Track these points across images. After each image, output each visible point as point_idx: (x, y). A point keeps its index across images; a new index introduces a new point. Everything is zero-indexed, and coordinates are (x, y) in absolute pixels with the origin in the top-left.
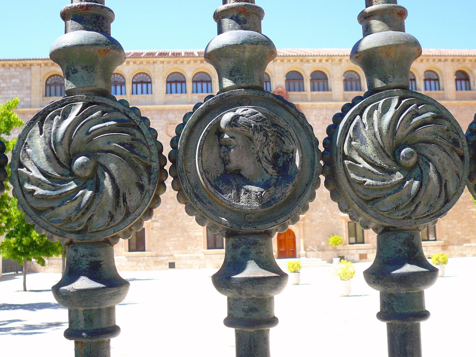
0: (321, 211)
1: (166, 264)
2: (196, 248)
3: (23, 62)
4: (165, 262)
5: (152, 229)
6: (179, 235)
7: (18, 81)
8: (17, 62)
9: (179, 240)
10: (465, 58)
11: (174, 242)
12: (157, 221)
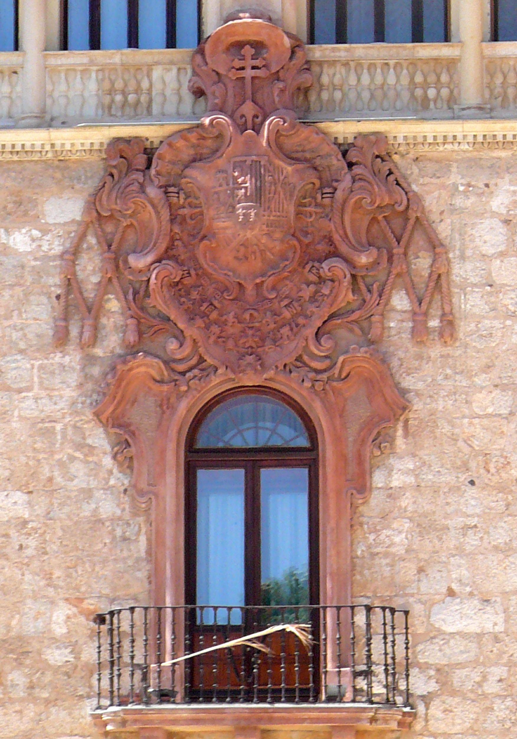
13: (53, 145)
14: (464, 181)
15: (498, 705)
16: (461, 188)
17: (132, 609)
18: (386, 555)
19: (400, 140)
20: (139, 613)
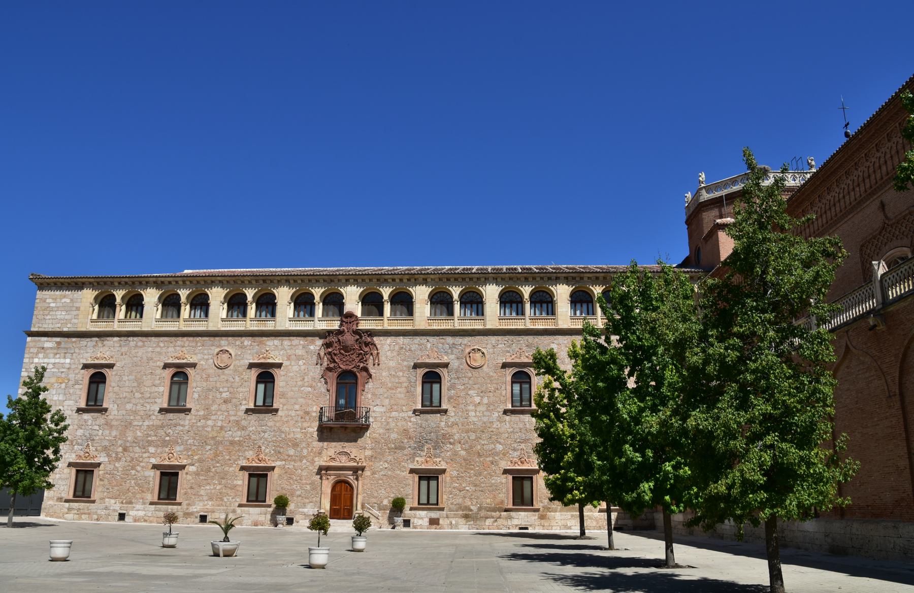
0: (386, 461)
1: (196, 517)
2: (234, 500)
3: (75, 280)
4: (196, 515)
5: (187, 474)
6: (216, 482)
7: (68, 301)
8: (69, 281)
9: (215, 489)
10: (582, 275)
11: (209, 491)
12: (193, 465)
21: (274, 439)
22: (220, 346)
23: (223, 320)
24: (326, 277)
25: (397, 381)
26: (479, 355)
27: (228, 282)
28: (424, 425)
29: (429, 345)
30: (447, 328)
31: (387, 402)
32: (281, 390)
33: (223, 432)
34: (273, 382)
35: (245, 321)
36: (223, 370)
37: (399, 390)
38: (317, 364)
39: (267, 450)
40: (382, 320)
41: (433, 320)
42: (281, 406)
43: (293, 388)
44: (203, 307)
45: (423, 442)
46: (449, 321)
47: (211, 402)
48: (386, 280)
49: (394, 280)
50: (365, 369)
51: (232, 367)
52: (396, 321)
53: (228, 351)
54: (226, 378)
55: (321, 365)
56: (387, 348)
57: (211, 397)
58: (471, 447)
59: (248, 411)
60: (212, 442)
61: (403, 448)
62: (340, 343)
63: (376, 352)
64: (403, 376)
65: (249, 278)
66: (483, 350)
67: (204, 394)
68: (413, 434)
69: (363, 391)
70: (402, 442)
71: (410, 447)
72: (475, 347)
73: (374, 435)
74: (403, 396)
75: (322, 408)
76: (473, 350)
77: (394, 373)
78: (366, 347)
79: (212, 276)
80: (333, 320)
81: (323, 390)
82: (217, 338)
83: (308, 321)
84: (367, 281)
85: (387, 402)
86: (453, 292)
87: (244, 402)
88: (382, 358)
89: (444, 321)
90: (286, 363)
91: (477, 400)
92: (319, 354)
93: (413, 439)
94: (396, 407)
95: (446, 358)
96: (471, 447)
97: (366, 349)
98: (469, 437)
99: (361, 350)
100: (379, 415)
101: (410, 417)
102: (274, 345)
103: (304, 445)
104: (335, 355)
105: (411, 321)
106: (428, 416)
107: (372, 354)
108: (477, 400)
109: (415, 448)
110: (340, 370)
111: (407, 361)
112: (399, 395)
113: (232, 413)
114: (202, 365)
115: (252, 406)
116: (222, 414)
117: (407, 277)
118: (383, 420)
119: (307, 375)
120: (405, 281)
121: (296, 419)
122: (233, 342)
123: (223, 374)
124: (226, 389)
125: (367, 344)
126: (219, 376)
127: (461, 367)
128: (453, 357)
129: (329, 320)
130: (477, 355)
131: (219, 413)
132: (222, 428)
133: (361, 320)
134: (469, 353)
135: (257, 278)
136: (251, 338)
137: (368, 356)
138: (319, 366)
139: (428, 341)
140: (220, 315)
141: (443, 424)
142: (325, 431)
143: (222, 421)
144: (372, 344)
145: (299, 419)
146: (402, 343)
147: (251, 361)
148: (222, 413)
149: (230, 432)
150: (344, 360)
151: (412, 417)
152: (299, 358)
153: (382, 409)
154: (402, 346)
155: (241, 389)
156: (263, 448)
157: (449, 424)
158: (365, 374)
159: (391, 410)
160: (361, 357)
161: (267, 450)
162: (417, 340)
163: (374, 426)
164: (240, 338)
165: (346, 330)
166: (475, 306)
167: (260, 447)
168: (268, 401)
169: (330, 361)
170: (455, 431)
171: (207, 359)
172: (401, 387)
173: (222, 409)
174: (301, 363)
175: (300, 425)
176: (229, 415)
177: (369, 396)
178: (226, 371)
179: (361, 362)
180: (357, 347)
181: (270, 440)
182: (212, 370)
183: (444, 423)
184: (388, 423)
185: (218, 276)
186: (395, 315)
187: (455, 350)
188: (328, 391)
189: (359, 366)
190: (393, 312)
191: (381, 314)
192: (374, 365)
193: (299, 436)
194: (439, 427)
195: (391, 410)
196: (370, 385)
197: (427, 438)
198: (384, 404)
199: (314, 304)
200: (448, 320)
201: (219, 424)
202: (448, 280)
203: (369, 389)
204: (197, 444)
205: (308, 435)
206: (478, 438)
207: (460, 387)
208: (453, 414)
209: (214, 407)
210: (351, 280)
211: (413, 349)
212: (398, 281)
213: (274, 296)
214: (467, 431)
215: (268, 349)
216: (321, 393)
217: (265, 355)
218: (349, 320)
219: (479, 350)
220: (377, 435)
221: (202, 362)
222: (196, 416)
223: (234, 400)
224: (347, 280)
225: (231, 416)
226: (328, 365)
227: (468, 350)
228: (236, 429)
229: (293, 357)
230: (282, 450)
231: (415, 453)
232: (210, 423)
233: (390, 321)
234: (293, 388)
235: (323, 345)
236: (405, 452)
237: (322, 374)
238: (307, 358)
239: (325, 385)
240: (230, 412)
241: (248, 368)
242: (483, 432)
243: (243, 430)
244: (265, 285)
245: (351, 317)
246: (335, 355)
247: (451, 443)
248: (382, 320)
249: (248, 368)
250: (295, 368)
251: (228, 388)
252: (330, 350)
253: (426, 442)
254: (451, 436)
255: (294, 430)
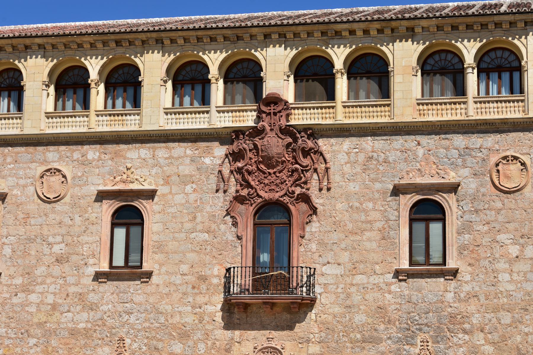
13: (216, 133)
14: (335, 142)
15: (341, 295)
16: (334, 144)
17: (238, 267)
18: (310, 251)
19: (316, 130)
20: (240, 269)
21: (147, 324)
22: (45, 162)
23: (49, 116)
24: (228, 32)
25: (363, 218)
26: (515, 167)
27: (54, 46)
28: (414, 299)
29: (420, 152)
30: (454, 118)
31: (345, 257)
32: (155, 238)
33: (57, 314)
34: (142, 224)
35: (87, 116)
36: (53, 205)
37: (368, 234)
38: (217, 191)
39: (135, 345)
40: (333, 107)
41: (427, 104)
42: (157, 266)
43: (177, 235)
44: (13, 93)
45: (414, 329)
46: (458, 106)
47: (34, 261)
48: (338, 33)
49: (352, 32)
50: (305, 198)
51: (67, 199)
52: (359, 109)
53: (59, 171)
54: (58, 218)
55: (225, 192)
56: (342, 158)
57: (33, 253)
58: (504, 338)
59: (98, 276)
60: (39, 332)
61: (380, 341)
62: (258, 153)
63: (323, 166)
64: (374, 209)
65: (91, 39)
66: (524, 158)
67: (22, 247)
68: (394, 316)
69: (303, 237)
70: (376, 330)
71: (389, 338)
72: (508, 153)
73: (323, 317)
74: (374, 245)
75: (228, 270)
76: (505, 158)
77: (357, 204)
78: (305, 157)
79: (26, 37)
80: (243, 111)
81: (231, 237)
82: (40, 149)
83: (199, 113)
84: (304, 35)
85: (345, 257)
86: (464, 51)
87: (91, 261)
88: (335, 177)
89: (448, 106)
90: (162, 190)
91: (514, 250)
92: (220, 172)
93: (394, 324)
94: (362, 266)
95: (452, 174)
96: (504, 338)
97: (306, 162)
98: (499, 320)
99: (297, 163)
100: (332, 281)
101: (388, 284)
102: (139, 157)
103: (199, 335)
104: (250, 173)
105: (387, 108)
106: (422, 282)
107: (316, 170)
108: (514, 250)
109: (399, 340)
110: (260, 200)
111: (381, 182)
112: (368, 245)
113: (71, 280)
114: (16, 196)
115: (105, 267)
116: (55, 283)
117: (377, 25)
118: (339, 290)
119: (201, 211)
120: (374, 33)
121: (183, 288)
122: (68, 154)
123: (53, 211)
124: (59, 239)
125: (306, 153)
126: (45, 215)
127: (482, 190)
128: (466, 172)
129: (236, 111)
130: (512, 167)
131: (48, 281)
132: (54, 307)
133: (294, 108)
134: (497, 165)
135: (105, 38)
136: (98, 146)
137: (308, 174)
138: (221, 194)
139: (419, 144)
140: (44, 107)
141: (450, 296)
142: (236, 310)
143: (55, 294)
144: (315, 153)
145: (189, 289)
146: (370, 149)
147: (101, 188)
148: (54, 280)
149: (70, 315)
150: (266, 181)
151: (391, 284)
152: (185, 180)
153: (339, 271)
154: (370, 154)
155: (85, 238)
156: (128, 341)
157: (462, 295)
158: (303, 206)
159: (354, 271)
160: (296, 175)
161: (135, 345)
162: (399, 141)
163: (323, 300)
164: (79, 147)
165: (268, 128)
166: (506, 76)
167: (122, 339)
168: (134, 258)
169: (241, 185)
170: (472, 308)
171: (25, 186)
172: (371, 230)
173: (54, 274)
174: (189, 188)
175: (191, 299)
176: (66, 284)
177: (314, 246)
178: (58, 206)
179: (297, 185)
180: (288, 157)
181: (140, 328)
182: (35, 206)
183: (452, 294)
184: (348, 296)
185: (37, 36)
186: (357, 97)
187: (469, 159)
188: (239, 238)
189: (293, 192)
190: (353, 92)
191: (331, 96)
192: (321, 190)
193: (189, 319)
194: (442, 302)
195: (354, 271)
196: (314, 227)
197: (420, 322)
198: (341, 261)
199: (209, 81)
200: (455, 103)
201: (50, 299)
202: (454, 28)
203: (312, 233)
204: (13, 336)
205: (206, 318)
206: (516, 323)
207: (480, 228)
208: (468, 278)
209: (41, 270)
210: (273, 36)
211: (391, 159)
212: (360, 33)
213: (136, 70)
214: (496, 310)
215: (129, 165)
216: (227, 243)
217: (125, 176)
218: (272, 109)
219: (516, 158)
220: (330, 318)
221: (15, 192)
222: (8, 286)
223: (74, 258)
224: (267, 36)
225: (70, 285)
226: (237, 191)
227: (494, 159)
228: (79, 308)
229: (174, 178)
230: (160, 345)
231: (399, 350)
232: (33, 298)
233: (347, 110)
234: (177, 235)
235: (226, 155)
236: (382, 347)
237: (226, 208)
238: (200, 180)
239: (233, 229)
240: (68, 278)
241: (96, 200)
242: (526, 310)
243: (92, 309)
244: (120, 50)
245: (276, 103)
246: (250, 173)
247: (465, 332)
248: (333, 107)
249: (96, 200)
250: (179, 199)
251: (63, 236)
252: (240, 165)
253: (420, 330)
254: (466, 317)
255: (180, 309)
